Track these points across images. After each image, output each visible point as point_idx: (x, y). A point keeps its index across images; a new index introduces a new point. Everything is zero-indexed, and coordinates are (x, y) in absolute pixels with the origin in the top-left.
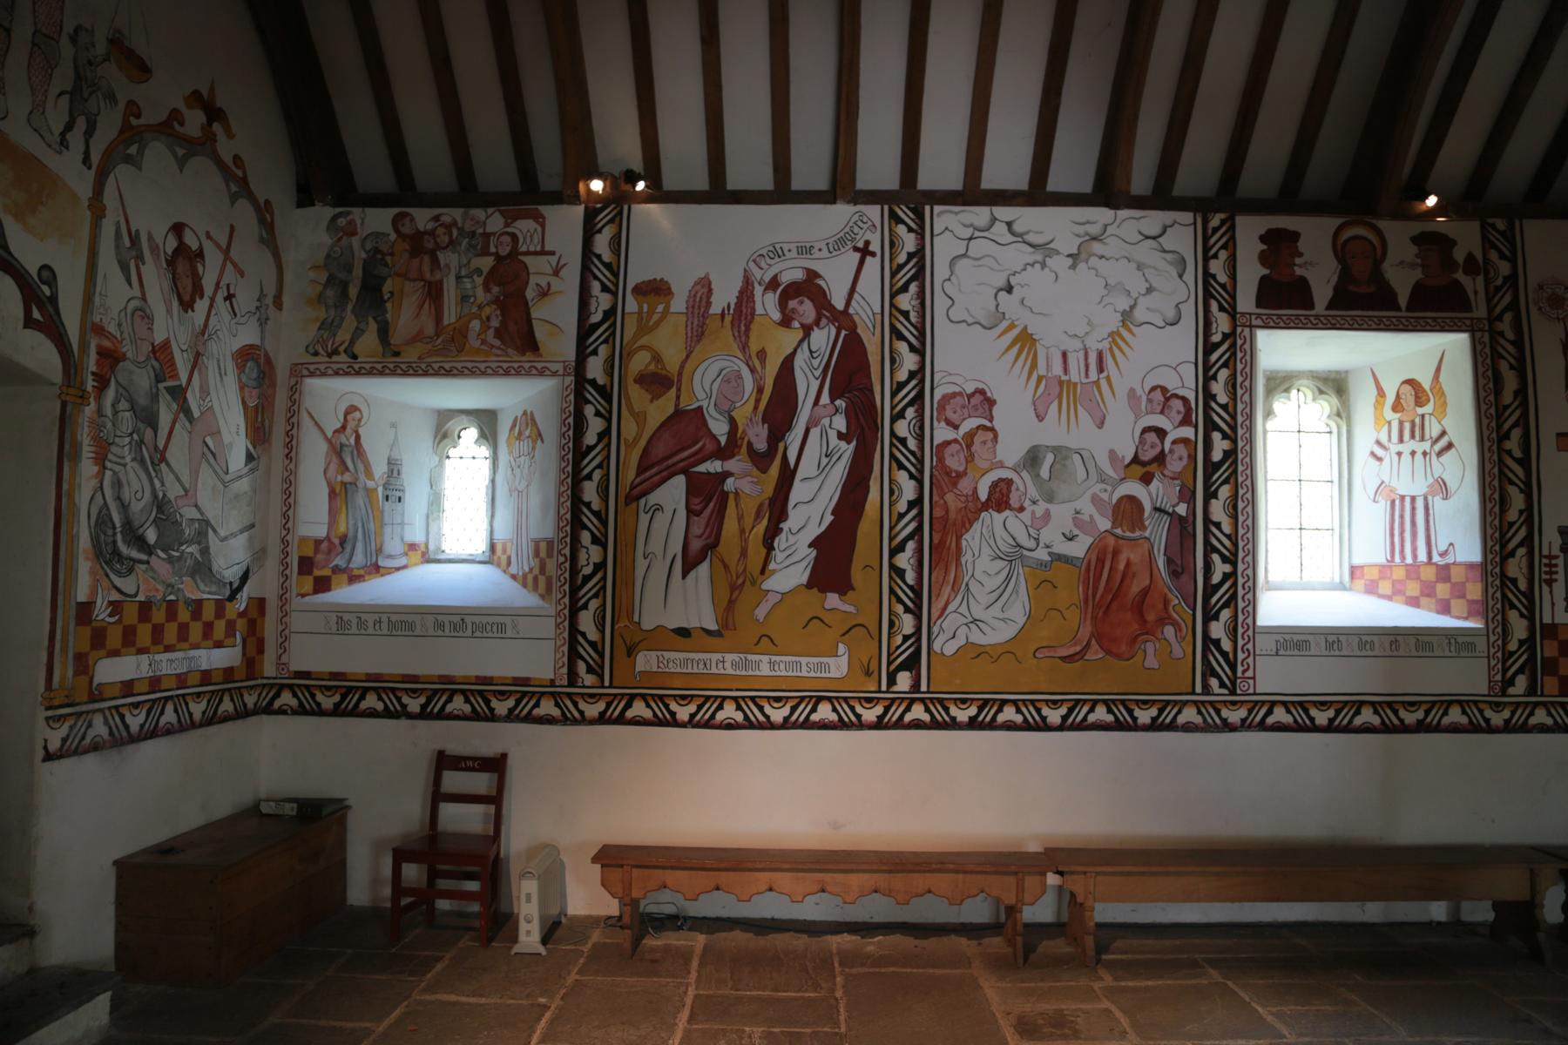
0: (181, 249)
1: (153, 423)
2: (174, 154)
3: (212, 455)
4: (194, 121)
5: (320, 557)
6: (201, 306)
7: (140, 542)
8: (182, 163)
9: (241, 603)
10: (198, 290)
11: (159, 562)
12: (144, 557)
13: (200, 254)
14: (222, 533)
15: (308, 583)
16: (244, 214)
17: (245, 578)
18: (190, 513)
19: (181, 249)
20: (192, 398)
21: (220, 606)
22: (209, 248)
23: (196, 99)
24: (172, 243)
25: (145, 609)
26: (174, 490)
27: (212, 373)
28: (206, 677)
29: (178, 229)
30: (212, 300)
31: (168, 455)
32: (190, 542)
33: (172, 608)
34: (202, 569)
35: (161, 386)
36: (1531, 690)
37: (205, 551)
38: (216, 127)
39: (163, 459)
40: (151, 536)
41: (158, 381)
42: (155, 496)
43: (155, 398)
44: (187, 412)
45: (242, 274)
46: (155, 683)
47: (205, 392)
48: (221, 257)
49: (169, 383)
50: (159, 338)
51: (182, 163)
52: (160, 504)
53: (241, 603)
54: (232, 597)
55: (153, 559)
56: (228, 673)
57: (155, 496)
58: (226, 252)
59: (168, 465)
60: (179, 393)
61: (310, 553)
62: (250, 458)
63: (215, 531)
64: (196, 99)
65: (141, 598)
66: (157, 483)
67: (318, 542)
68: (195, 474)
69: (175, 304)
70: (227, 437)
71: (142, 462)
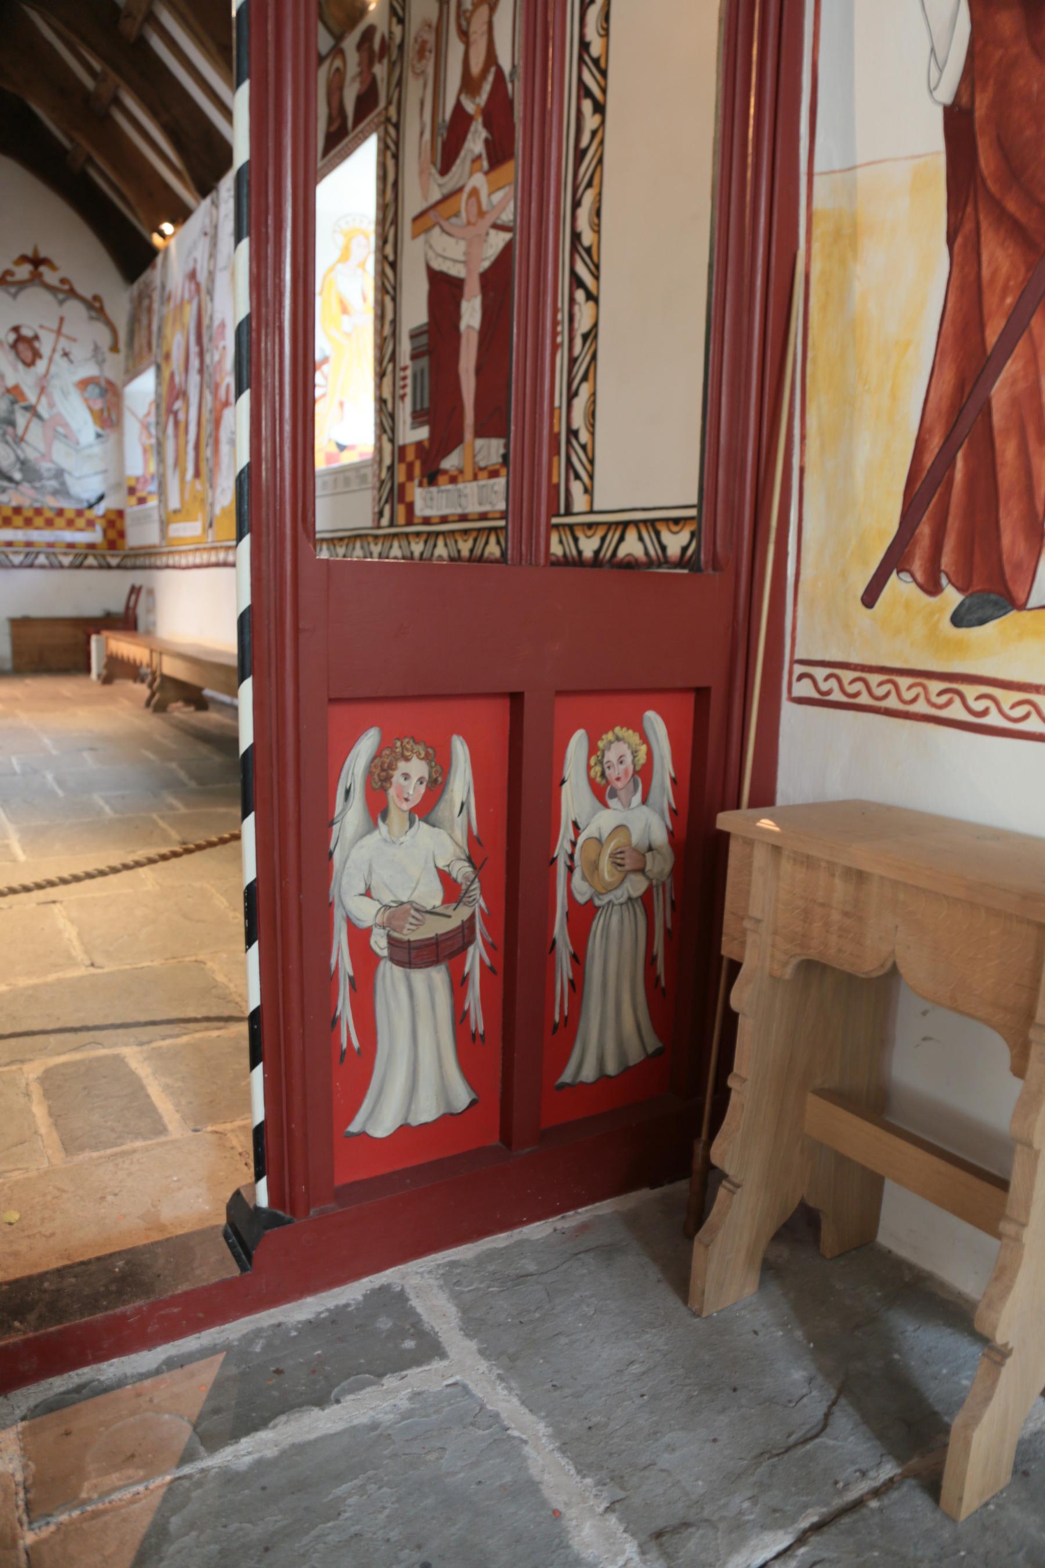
0: (20, 339)
1: (12, 423)
2: (9, 293)
3: (69, 438)
4: (24, 271)
5: (139, 487)
6: (41, 365)
7: (10, 479)
8: (15, 296)
9: (100, 509)
10: (37, 355)
11: (25, 487)
12: (12, 485)
13: (36, 337)
14: (77, 474)
15: (133, 500)
16: (74, 310)
17: (101, 498)
18: (45, 466)
19: (20, 339)
20: (43, 410)
21: (80, 513)
22: (42, 334)
23: (24, 259)
24: (12, 337)
25: (17, 510)
26: (31, 454)
27: (57, 396)
28: (71, 546)
29: (16, 329)
30: (51, 360)
31: (28, 437)
32: (49, 479)
33: (38, 512)
34: (62, 491)
35: (17, 407)
36: (392, 524)
37: (63, 484)
38: (43, 269)
39: (22, 439)
40: (17, 476)
41: (13, 402)
42: (18, 458)
43: (12, 412)
44: (39, 417)
45: (74, 340)
46: (29, 544)
47: (51, 405)
48: (53, 336)
49: (23, 404)
50: (10, 382)
51: (15, 296)
52: (23, 464)
53: (100, 509)
54: (91, 506)
55: (20, 487)
56: (91, 546)
57: (18, 458)
58: (59, 332)
59: (28, 444)
60: (31, 409)
61: (133, 483)
62: (99, 436)
63: (70, 474)
64: (24, 259)
65: (14, 504)
66: (19, 452)
67: (137, 479)
68: (49, 446)
69: (20, 366)
70: (74, 425)
71: (7, 443)
